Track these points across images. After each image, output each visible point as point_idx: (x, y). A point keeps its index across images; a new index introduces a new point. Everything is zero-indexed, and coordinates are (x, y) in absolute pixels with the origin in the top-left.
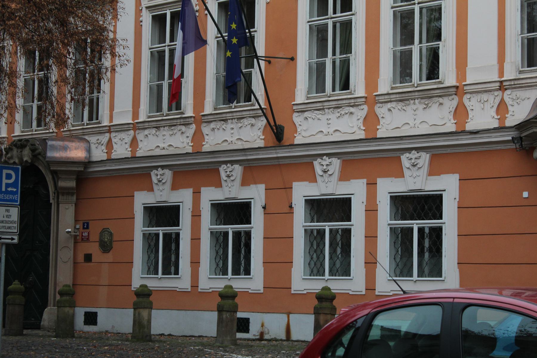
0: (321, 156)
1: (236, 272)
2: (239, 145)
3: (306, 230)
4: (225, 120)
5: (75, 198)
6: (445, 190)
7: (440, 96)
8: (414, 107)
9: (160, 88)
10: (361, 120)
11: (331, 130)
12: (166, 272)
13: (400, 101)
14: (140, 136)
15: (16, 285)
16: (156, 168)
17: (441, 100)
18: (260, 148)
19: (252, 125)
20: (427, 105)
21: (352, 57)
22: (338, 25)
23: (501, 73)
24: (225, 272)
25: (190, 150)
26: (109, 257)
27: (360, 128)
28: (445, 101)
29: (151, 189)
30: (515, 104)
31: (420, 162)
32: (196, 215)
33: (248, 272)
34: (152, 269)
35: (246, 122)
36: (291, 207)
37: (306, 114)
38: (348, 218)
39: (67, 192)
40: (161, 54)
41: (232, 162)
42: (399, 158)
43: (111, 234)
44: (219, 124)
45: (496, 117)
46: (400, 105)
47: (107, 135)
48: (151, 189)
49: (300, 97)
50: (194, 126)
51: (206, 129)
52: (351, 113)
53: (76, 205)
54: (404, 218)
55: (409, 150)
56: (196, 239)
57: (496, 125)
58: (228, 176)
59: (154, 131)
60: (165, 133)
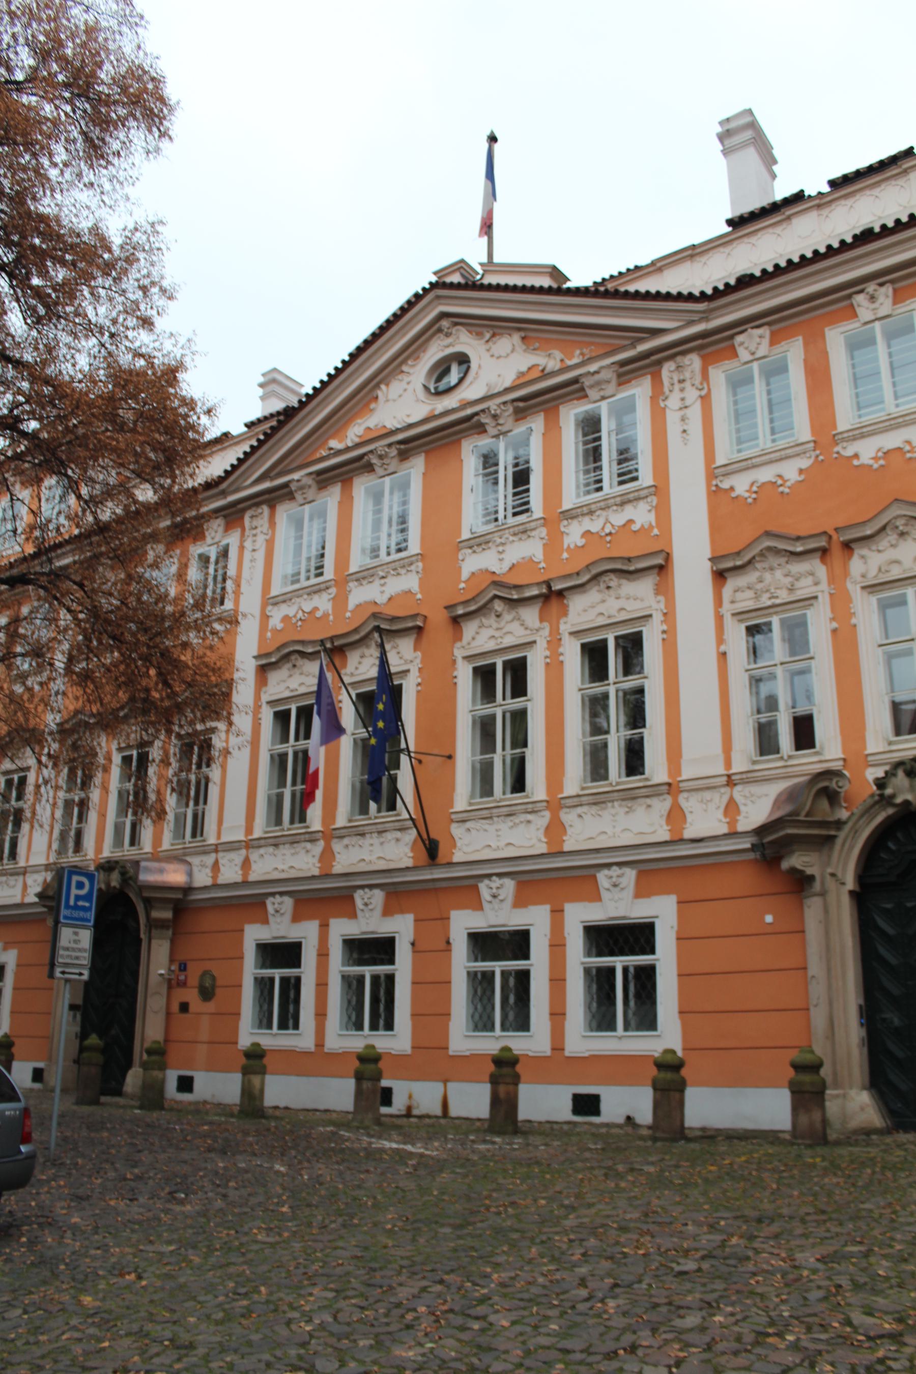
0: (489, 876)
1: (374, 1027)
2: (382, 865)
3: (469, 973)
4: (363, 835)
5: (170, 932)
6: (657, 917)
7: (647, 797)
8: (613, 811)
9: (280, 797)
10: (542, 831)
11: (502, 844)
12: (283, 1025)
13: (595, 804)
14: (254, 856)
15: (93, 1040)
16: (273, 894)
17: (648, 801)
18: (407, 868)
19: (398, 840)
20: (629, 808)
21: (528, 752)
22: (508, 715)
23: (728, 763)
24: (359, 1026)
25: (316, 872)
26: (211, 1006)
27: (540, 840)
28: (654, 801)
29: (266, 921)
30: (749, 802)
31: (624, 881)
32: (323, 954)
33: (389, 1026)
34: (265, 1021)
35: (389, 836)
36: (448, 943)
37: (469, 825)
38: (526, 957)
39: (162, 925)
40: (283, 757)
41: (371, 887)
42: (594, 877)
43: (214, 978)
44: (354, 840)
45: (724, 820)
46: (594, 809)
47: (213, 855)
48: (266, 921)
49: (461, 802)
50: (322, 843)
51: (337, 846)
52: (529, 822)
53: (173, 942)
54: (600, 954)
55: (608, 866)
56: (322, 985)
57: (724, 830)
58: (366, 904)
59: (271, 849)
60: (285, 851)
